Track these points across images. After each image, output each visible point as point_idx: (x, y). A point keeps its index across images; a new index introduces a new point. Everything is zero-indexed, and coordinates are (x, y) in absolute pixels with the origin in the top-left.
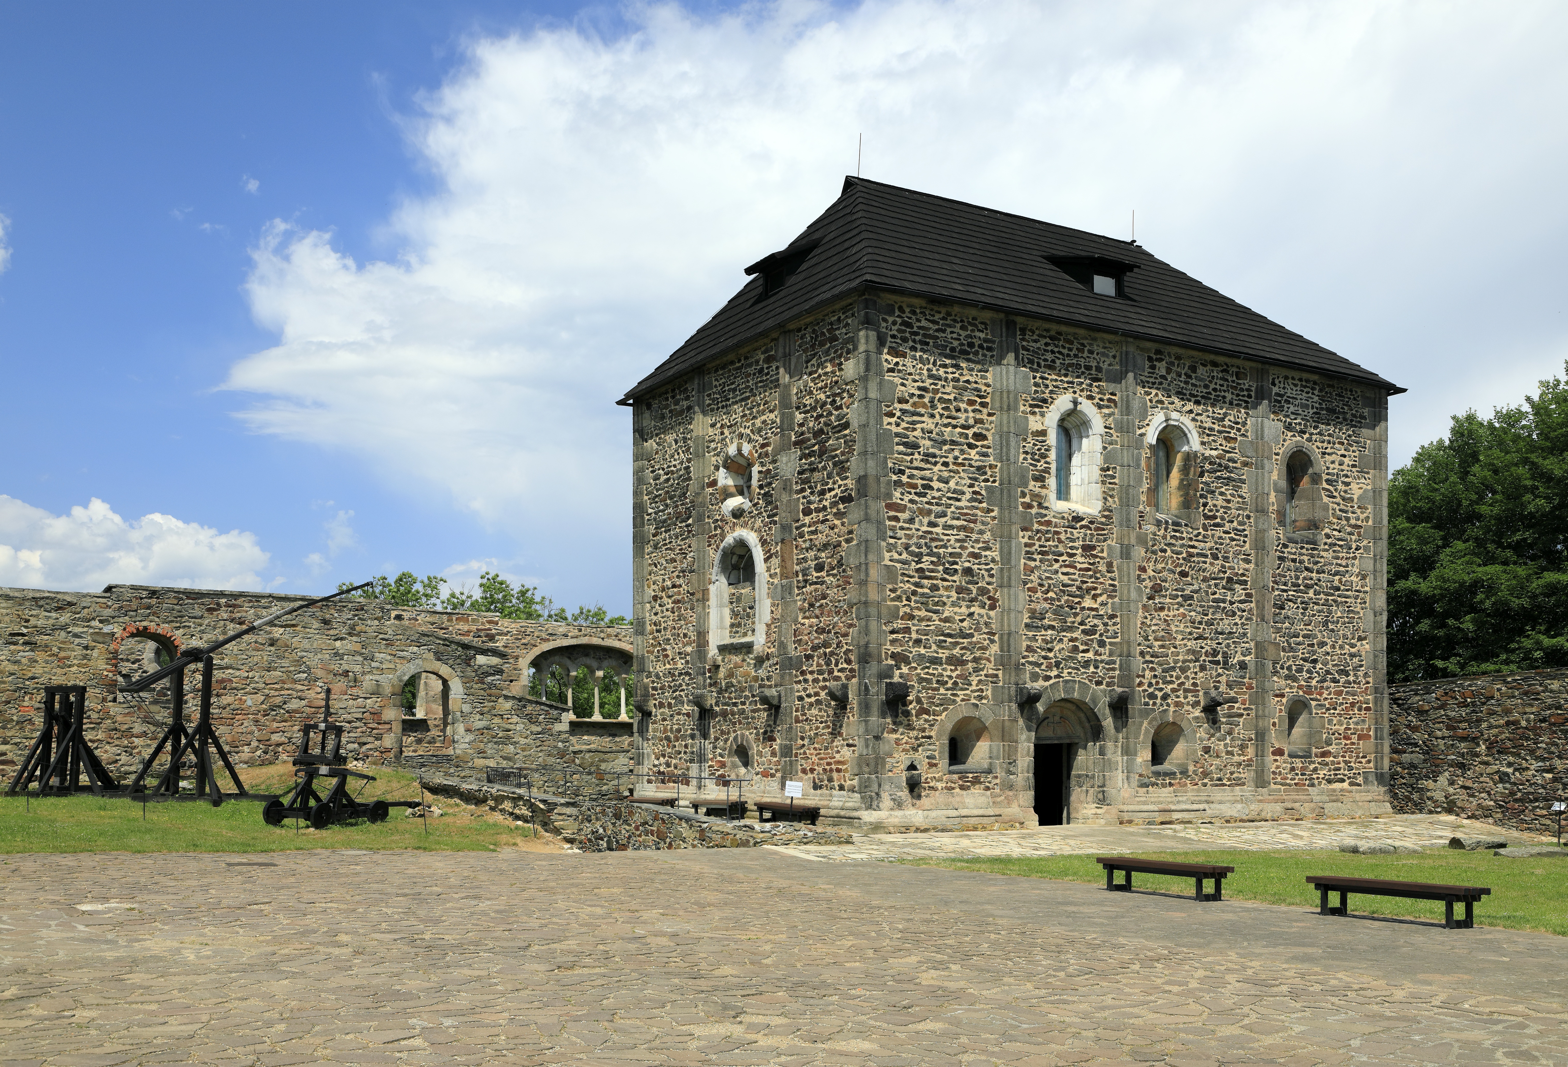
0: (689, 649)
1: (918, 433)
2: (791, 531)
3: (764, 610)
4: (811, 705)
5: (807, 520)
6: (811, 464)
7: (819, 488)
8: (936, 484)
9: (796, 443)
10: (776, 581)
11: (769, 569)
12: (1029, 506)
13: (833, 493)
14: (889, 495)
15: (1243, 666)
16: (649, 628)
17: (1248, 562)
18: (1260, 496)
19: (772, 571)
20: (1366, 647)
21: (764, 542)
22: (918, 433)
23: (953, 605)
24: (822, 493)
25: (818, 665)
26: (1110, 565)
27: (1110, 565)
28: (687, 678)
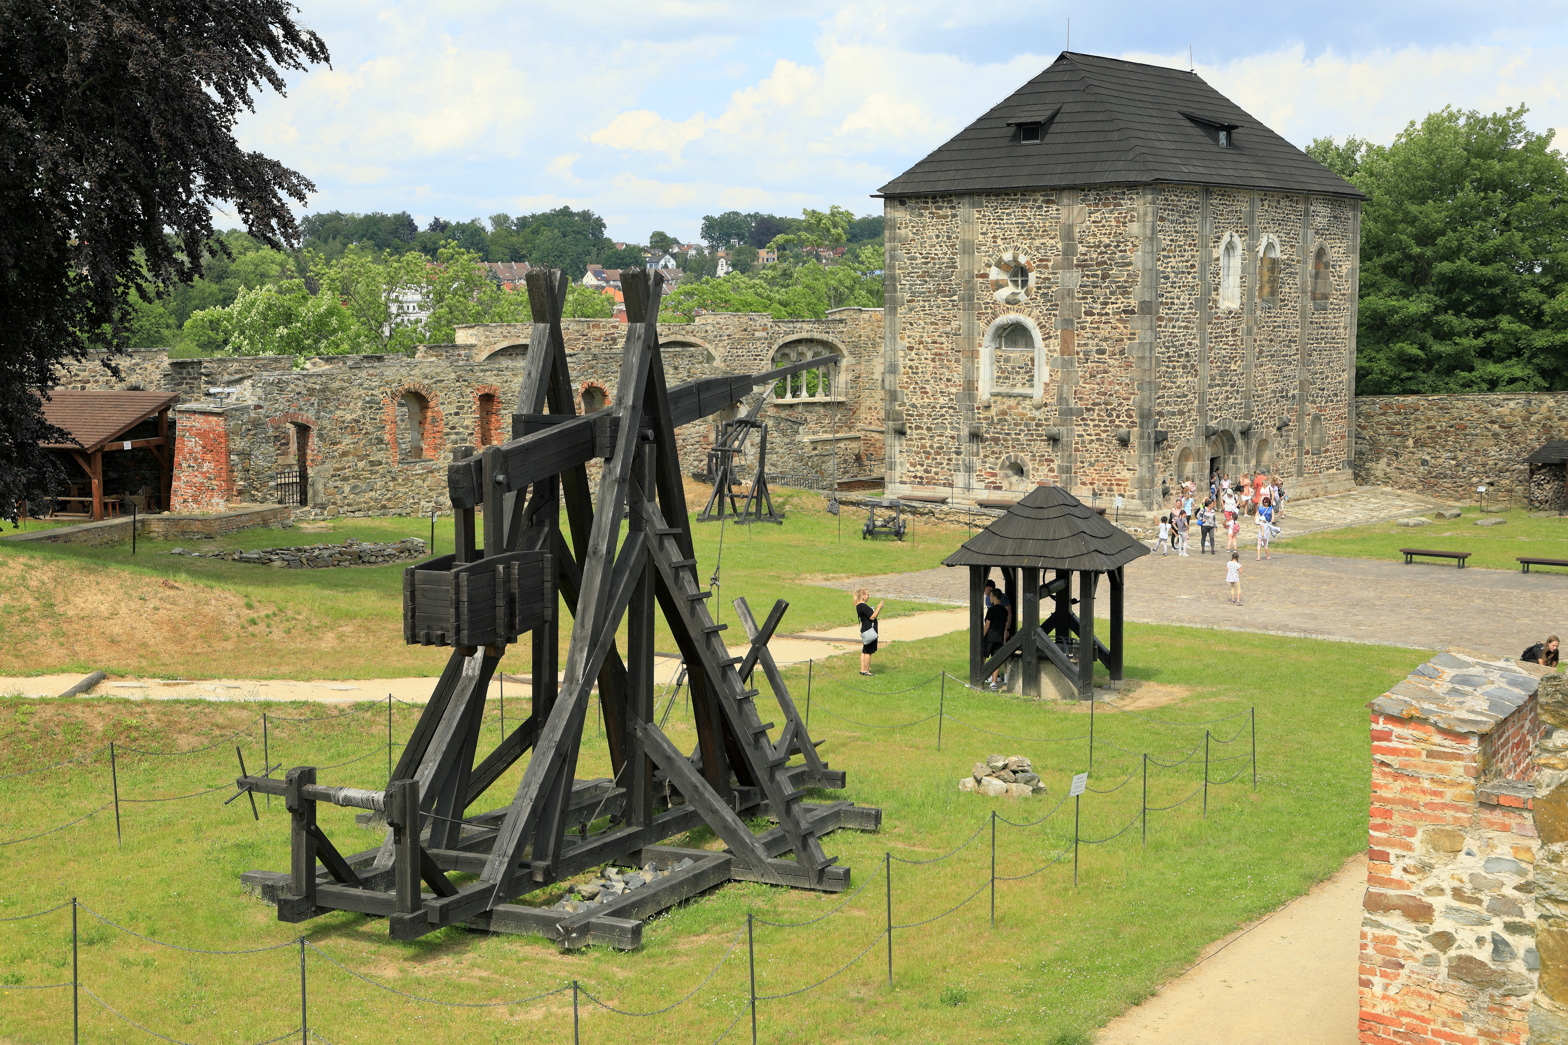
0: (953, 390)
1: (1169, 269)
2: (1072, 324)
3: (1043, 373)
4: (1092, 441)
5: (1089, 319)
6: (1094, 282)
7: (1101, 300)
8: (1176, 301)
9: (1077, 266)
10: (1055, 355)
11: (1047, 346)
12: (1211, 308)
13: (1115, 306)
14: (1158, 312)
15: (1294, 396)
16: (902, 370)
17: (1297, 327)
18: (1304, 283)
19: (1051, 348)
20: (1345, 376)
21: (1042, 327)
22: (1169, 269)
23: (1182, 376)
24: (1106, 304)
25: (1099, 415)
26: (1242, 340)
27: (1242, 340)
28: (951, 411)
